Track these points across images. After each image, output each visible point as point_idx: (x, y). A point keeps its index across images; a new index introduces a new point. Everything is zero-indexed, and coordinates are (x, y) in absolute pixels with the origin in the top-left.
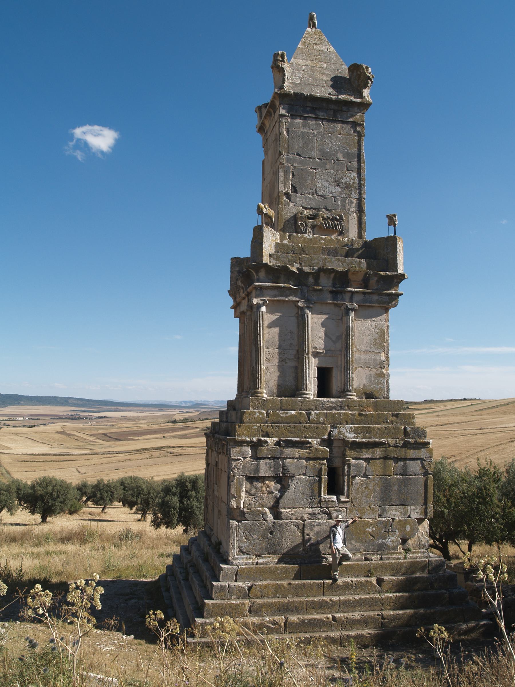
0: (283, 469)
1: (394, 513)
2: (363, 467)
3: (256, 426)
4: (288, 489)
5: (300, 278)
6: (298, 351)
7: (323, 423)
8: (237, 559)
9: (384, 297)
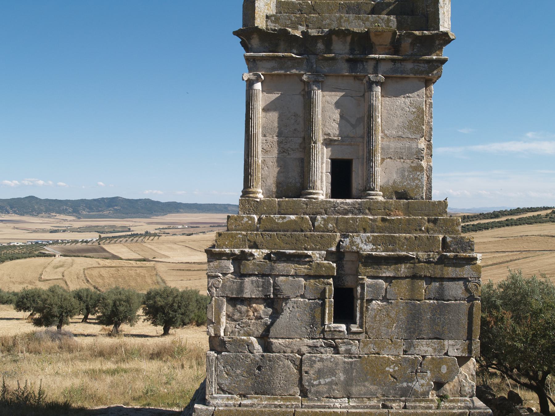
0: (274, 289)
1: (425, 348)
2: (382, 288)
3: (241, 234)
4: (281, 314)
5: (306, 44)
6: (304, 139)
7: (331, 231)
8: (216, 398)
9: (422, 65)
